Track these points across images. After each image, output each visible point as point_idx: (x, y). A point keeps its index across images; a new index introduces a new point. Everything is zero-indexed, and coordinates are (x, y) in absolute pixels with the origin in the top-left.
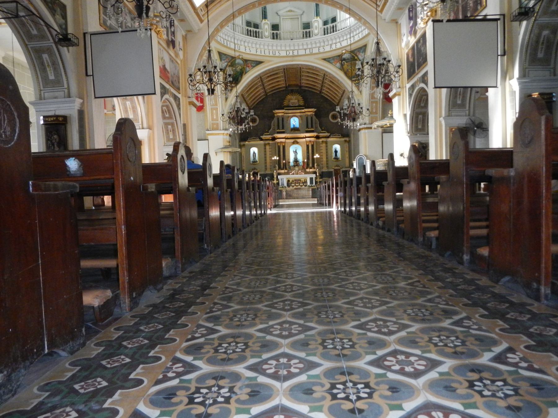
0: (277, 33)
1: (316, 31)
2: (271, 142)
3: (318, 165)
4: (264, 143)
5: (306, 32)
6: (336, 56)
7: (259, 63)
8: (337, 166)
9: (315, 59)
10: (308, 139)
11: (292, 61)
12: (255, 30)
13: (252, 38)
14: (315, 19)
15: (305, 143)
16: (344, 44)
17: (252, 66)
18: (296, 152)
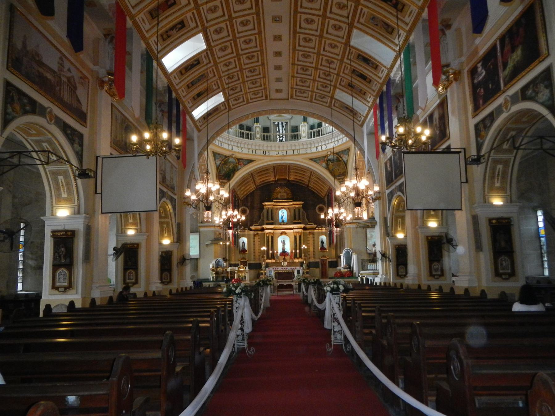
0: (267, 137)
1: (303, 135)
2: (260, 232)
3: (305, 256)
5: (295, 135)
7: (250, 161)
8: (324, 256)
9: (303, 159)
12: (247, 132)
13: (244, 139)
14: (303, 124)
15: (293, 234)
18: (284, 243)
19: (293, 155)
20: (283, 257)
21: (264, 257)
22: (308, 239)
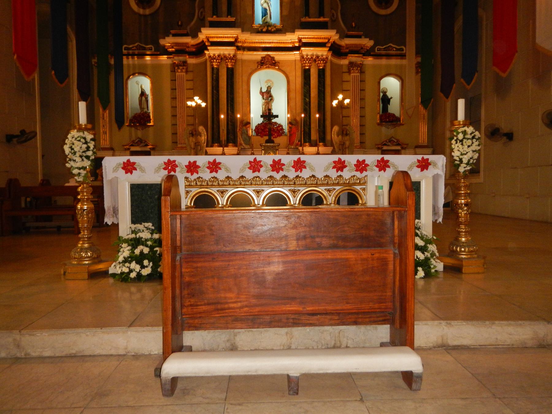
2: (191, 61)
3: (344, 132)
4: (170, 62)
10: (306, 51)
15: (299, 66)
18: (267, 96)
20: (266, 138)
21: (200, 134)
22: (346, 86)
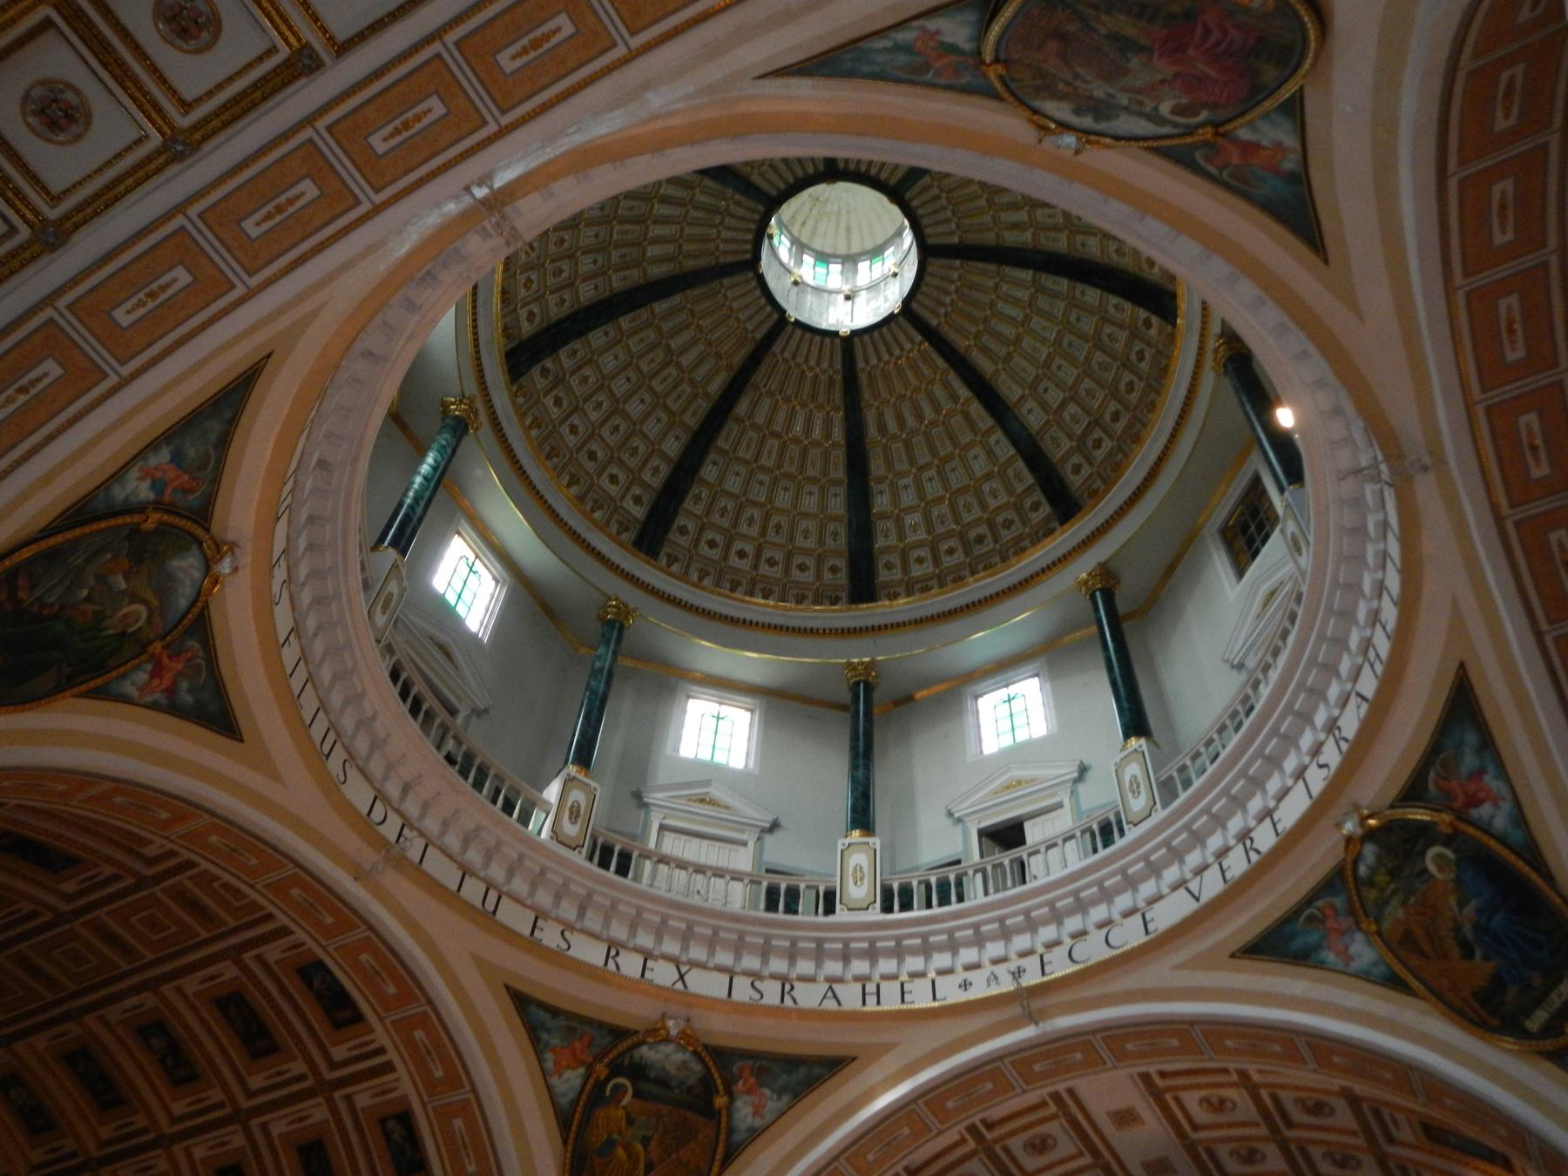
6: (601, 1025)
9: (479, 961)
11: (359, 875)
16: (706, 984)
17: (171, 691)
19: (452, 899)
